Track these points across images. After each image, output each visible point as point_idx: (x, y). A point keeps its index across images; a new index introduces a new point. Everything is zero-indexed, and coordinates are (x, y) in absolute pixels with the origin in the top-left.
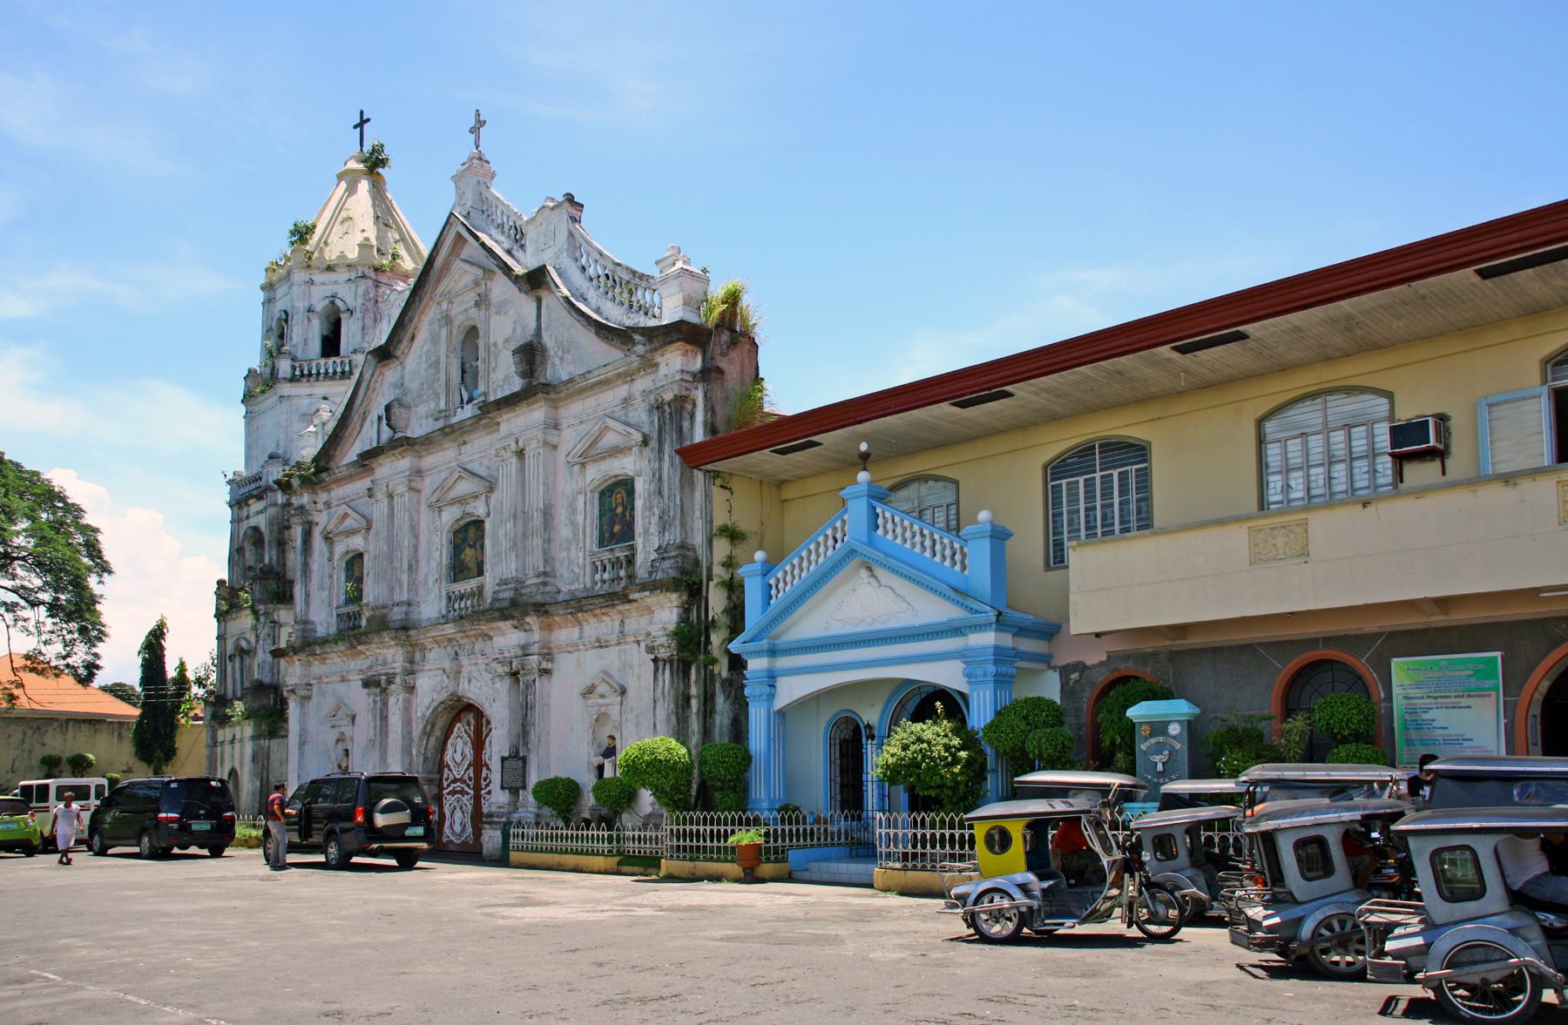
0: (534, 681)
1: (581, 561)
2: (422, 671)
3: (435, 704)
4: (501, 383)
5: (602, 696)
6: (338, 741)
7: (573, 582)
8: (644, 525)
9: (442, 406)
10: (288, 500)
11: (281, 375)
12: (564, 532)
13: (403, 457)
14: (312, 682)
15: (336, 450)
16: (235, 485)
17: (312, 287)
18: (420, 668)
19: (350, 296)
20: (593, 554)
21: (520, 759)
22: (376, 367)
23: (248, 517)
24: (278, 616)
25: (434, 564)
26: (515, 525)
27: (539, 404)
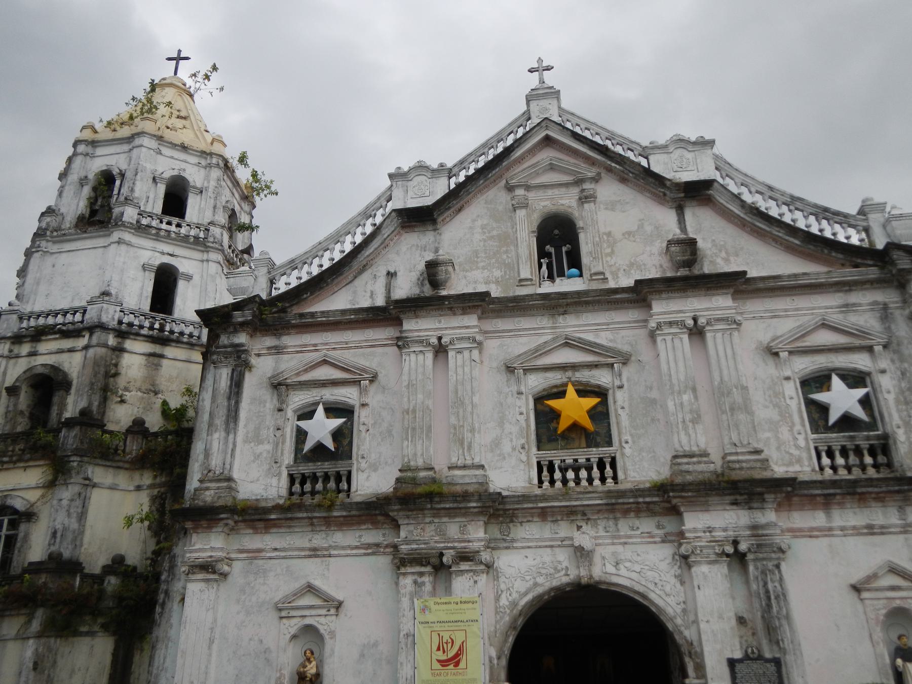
0: (778, 566)
1: (802, 443)
2: (507, 548)
3: (540, 590)
4: (625, 267)
5: (893, 588)
6: (294, 637)
7: (790, 464)
8: (901, 418)
9: (525, 273)
10: (119, 343)
11: (126, 218)
12: (764, 412)
13: (464, 314)
14: (233, 556)
15: (311, 294)
16: (15, 317)
17: (159, 156)
18: (505, 545)
19: (194, 175)
20: (815, 440)
21: (768, 661)
22: (398, 226)
23: (33, 354)
24: (93, 472)
25: (511, 428)
26: (696, 398)
27: (725, 291)
